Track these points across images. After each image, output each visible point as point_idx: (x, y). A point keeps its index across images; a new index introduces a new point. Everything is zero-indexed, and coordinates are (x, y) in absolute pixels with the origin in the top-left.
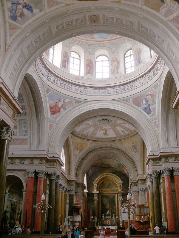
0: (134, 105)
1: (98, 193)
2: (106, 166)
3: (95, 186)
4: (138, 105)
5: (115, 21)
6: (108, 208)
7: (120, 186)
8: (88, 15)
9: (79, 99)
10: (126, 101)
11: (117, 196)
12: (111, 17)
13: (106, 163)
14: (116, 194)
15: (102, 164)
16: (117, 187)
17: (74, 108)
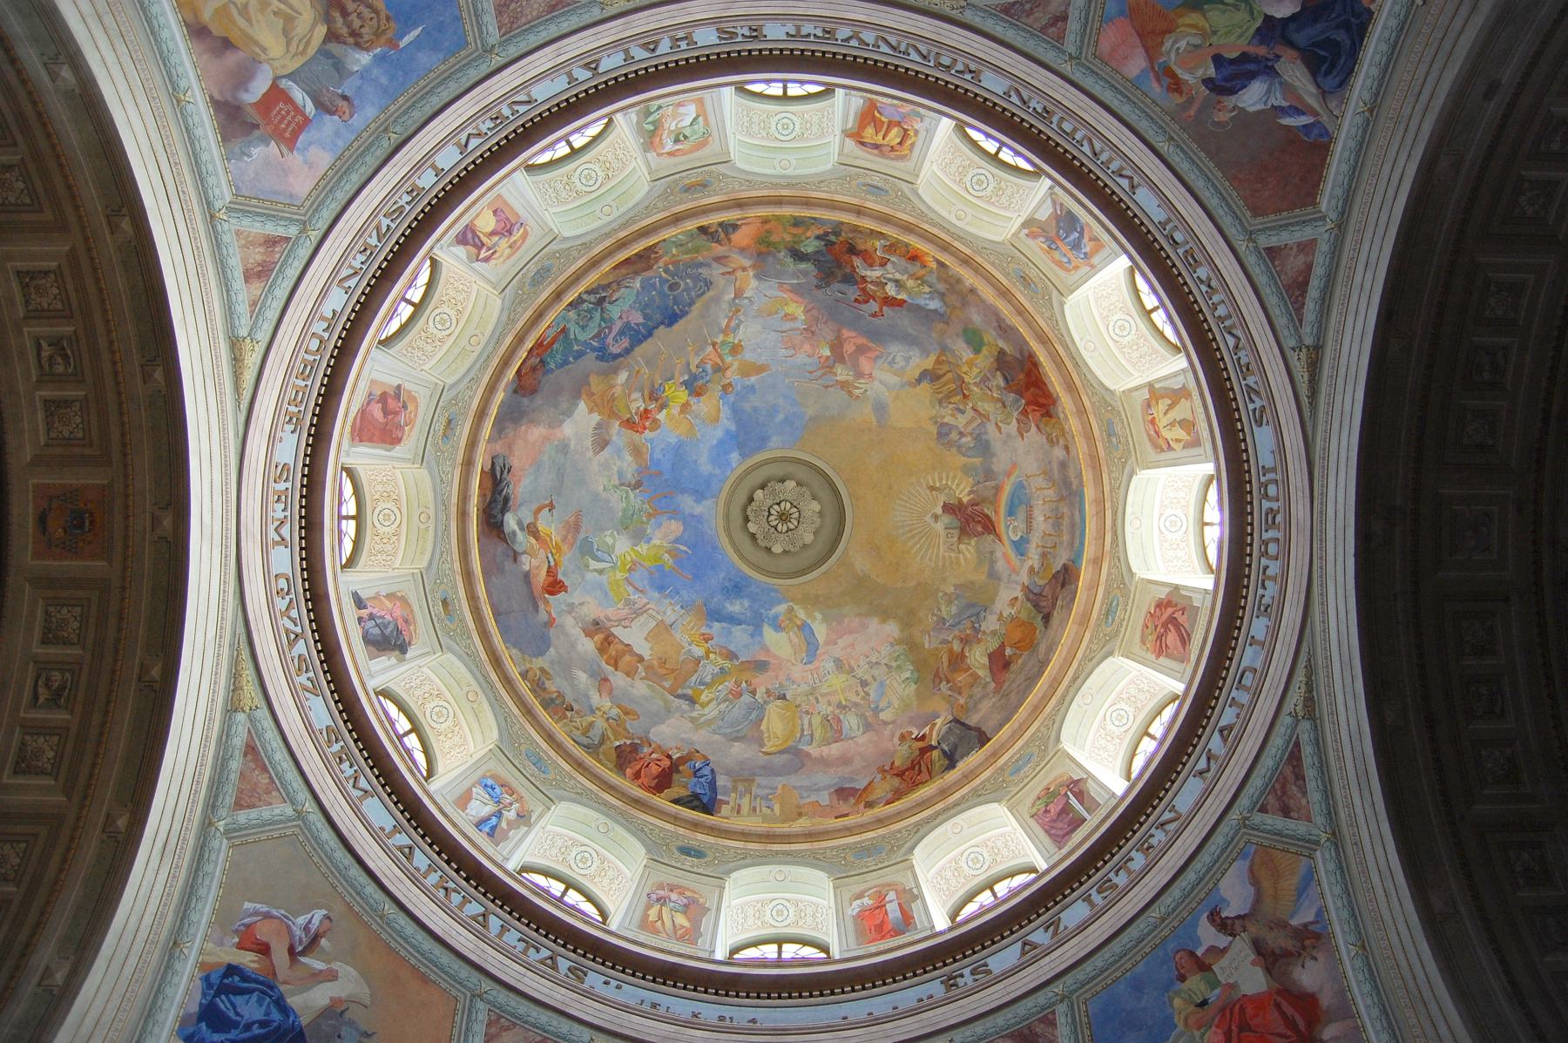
0: (1327, 200)
4: (1315, 147)
5: (71, 393)
8: (37, 555)
9: (1268, 762)
10: (1296, 289)
12: (40, 416)
17: (1336, 838)
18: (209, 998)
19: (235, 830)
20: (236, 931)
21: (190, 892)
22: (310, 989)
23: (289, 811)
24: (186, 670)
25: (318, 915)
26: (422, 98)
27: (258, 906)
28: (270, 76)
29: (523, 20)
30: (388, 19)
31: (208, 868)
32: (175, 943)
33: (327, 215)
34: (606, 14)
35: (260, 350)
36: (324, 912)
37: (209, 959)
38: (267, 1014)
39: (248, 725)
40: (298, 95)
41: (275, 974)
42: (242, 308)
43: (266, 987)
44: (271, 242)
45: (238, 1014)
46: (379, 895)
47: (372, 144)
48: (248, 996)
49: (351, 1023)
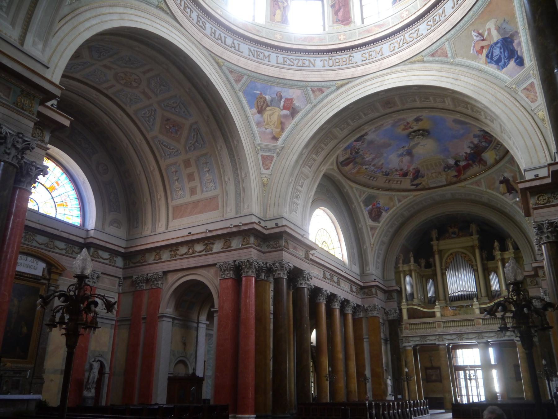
5: (361, 114)
12: (369, 115)
18: (493, 62)
19: (453, 57)
20: (478, 55)
21: (468, 67)
22: (492, 36)
23: (447, 43)
24: (414, 82)
25: (473, 33)
26: (267, 81)
27: (472, 49)
28: (282, 111)
29: (238, 75)
30: (257, 99)
31: (462, 63)
32: (480, 70)
33: (302, 83)
34: (225, 61)
35: (337, 82)
36: (472, 32)
37: (484, 61)
38: (498, 47)
39: (426, 57)
40: (282, 104)
41: (488, 45)
42: (330, 90)
43: (492, 47)
44: (313, 91)
45: (498, 55)
46: (467, 16)
47: (283, 84)
48: (494, 53)
49: (502, 25)
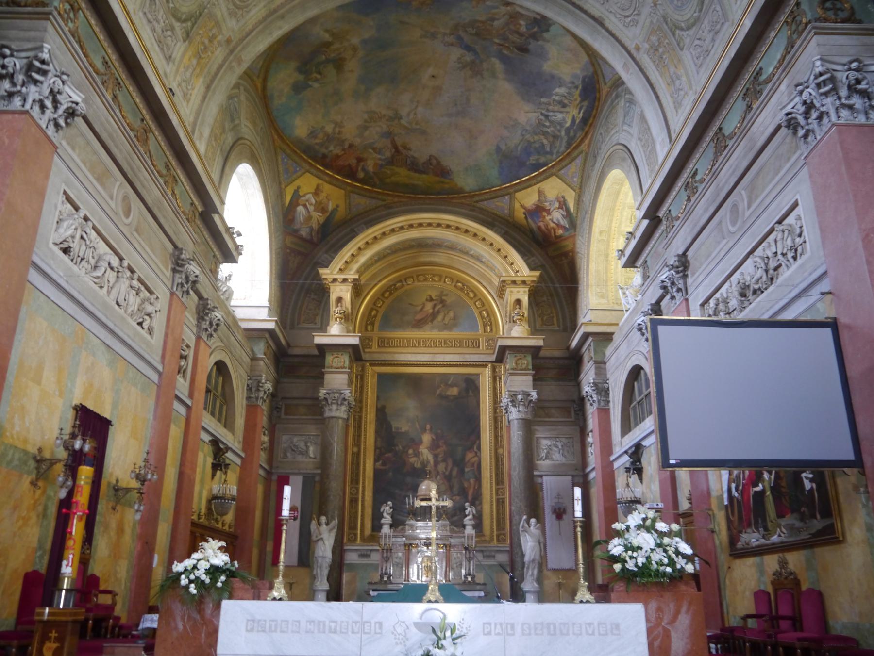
1: (355, 353)
2: (420, 180)
3: (333, 297)
6: (424, 464)
7: (518, 302)
11: (495, 378)
13: (420, 150)
14: (483, 365)
15: (391, 162)
16: (490, 321)
